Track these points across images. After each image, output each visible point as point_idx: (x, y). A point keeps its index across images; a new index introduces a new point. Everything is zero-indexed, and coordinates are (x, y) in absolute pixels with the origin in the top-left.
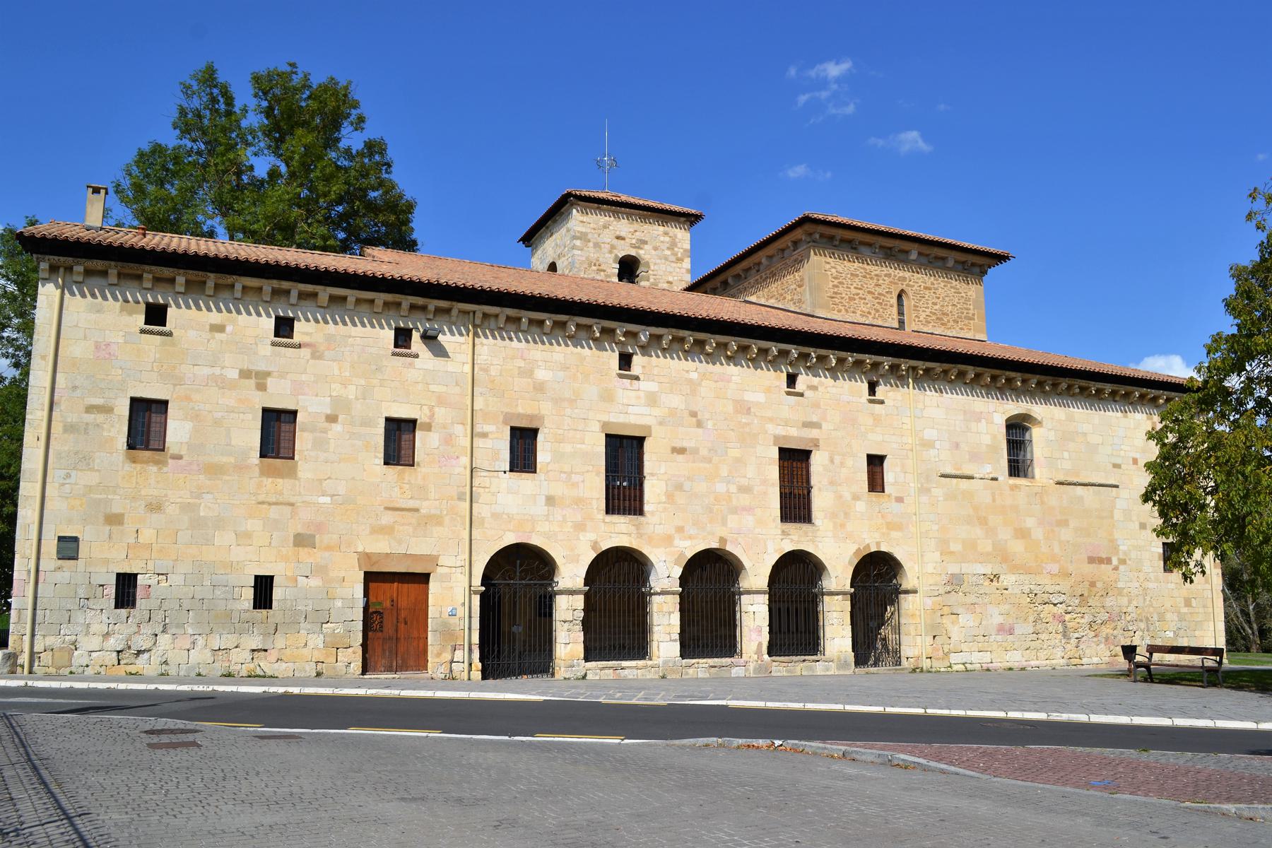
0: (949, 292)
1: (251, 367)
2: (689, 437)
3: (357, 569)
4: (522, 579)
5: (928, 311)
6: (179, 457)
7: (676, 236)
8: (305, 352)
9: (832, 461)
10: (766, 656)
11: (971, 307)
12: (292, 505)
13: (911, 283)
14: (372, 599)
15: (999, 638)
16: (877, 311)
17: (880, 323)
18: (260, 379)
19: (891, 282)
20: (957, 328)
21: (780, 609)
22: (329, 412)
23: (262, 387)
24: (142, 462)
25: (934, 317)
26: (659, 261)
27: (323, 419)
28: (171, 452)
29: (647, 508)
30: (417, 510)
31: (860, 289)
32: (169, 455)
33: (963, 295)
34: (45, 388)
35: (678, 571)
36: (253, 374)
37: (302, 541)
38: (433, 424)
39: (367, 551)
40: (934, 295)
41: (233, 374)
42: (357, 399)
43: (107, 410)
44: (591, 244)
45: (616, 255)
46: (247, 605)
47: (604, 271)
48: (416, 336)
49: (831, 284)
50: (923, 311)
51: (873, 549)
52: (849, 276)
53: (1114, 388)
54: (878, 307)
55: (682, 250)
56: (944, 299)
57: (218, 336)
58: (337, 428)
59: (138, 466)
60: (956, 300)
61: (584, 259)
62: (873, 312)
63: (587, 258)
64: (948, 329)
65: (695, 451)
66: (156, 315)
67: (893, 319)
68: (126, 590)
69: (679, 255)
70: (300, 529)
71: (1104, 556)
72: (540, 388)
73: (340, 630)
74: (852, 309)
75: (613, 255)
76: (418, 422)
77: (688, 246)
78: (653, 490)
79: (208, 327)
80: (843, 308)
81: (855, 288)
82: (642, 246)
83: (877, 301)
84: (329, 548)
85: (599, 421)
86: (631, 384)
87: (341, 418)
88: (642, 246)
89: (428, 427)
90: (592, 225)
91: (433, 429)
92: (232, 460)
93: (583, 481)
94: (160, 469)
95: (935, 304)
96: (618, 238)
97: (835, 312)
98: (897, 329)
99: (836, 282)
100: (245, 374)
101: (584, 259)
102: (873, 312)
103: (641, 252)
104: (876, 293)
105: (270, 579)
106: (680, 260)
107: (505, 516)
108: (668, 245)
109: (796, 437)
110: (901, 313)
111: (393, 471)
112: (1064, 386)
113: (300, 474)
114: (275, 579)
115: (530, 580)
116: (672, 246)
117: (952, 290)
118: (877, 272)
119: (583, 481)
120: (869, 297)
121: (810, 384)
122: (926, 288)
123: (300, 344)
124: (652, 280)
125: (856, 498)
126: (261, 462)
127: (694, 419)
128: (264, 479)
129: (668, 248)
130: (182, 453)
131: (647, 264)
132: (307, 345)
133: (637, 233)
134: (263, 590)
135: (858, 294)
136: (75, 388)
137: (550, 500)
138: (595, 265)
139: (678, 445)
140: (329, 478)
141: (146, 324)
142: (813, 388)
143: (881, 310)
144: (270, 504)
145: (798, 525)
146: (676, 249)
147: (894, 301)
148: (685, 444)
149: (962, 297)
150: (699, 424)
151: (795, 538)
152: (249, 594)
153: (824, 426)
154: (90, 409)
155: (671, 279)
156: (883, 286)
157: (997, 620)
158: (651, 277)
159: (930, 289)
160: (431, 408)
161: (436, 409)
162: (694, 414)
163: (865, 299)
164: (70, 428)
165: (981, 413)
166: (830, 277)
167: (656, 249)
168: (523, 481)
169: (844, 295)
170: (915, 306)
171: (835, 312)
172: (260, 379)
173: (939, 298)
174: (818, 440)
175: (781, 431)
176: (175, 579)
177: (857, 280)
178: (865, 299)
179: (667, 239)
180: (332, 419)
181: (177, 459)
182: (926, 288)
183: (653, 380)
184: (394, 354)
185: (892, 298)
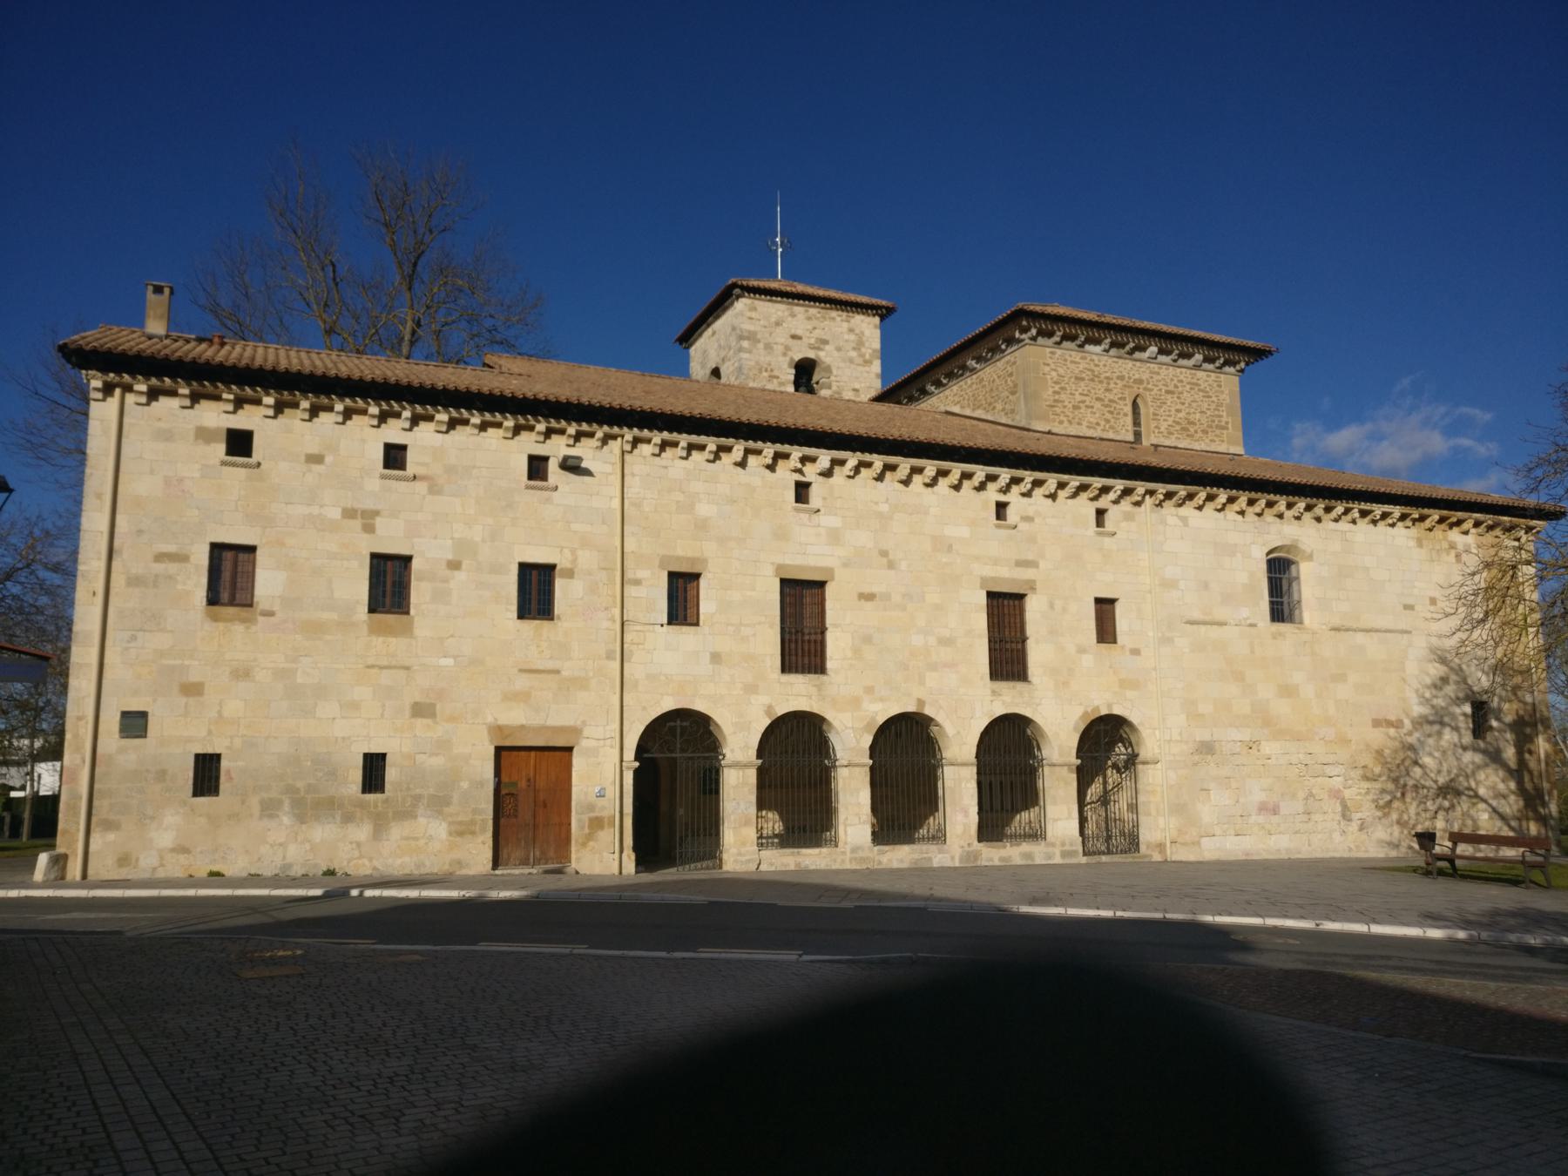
0: (1196, 396)
2: (878, 580)
4: (683, 750)
5: (1171, 419)
6: (270, 614)
7: (862, 333)
8: (421, 487)
9: (1052, 606)
11: (1225, 414)
12: (407, 668)
13: (1150, 386)
14: (505, 779)
15: (1261, 819)
16: (1108, 421)
18: (368, 520)
19: (1125, 386)
20: (1207, 441)
21: (991, 784)
22: (450, 557)
23: (369, 529)
25: (1178, 428)
26: (842, 365)
29: (829, 665)
30: (557, 672)
31: (1087, 395)
32: (258, 611)
33: (1214, 399)
34: (102, 532)
35: (868, 740)
36: (359, 512)
37: (422, 710)
38: (576, 570)
39: (500, 723)
40: (1178, 401)
41: (335, 513)
42: (483, 541)
43: (181, 558)
44: (761, 346)
45: (792, 359)
48: (553, 466)
49: (1051, 390)
50: (1165, 420)
51: (1104, 712)
52: (1073, 380)
53: (1404, 511)
54: (1108, 416)
56: (1190, 404)
57: (317, 468)
58: (460, 576)
59: (221, 625)
60: (1206, 405)
61: (752, 363)
62: (1103, 423)
63: (757, 363)
64: (1196, 441)
65: (887, 597)
66: (239, 443)
67: (1127, 431)
68: (207, 773)
69: (867, 357)
70: (418, 699)
71: (1393, 718)
72: (702, 525)
75: (788, 359)
76: (558, 568)
77: (877, 345)
78: (837, 645)
79: (303, 458)
80: (1065, 419)
81: (1081, 394)
82: (822, 346)
83: (1108, 409)
84: (452, 719)
85: (773, 564)
86: (810, 520)
88: (822, 346)
89: (570, 574)
90: (762, 322)
91: (576, 576)
92: (334, 616)
93: (754, 635)
94: (248, 628)
95: (1178, 411)
96: (794, 337)
97: (1056, 424)
98: (1132, 443)
99: (1057, 388)
100: (349, 513)
101: (752, 363)
103: (822, 354)
104: (1106, 400)
105: (382, 757)
106: (867, 362)
107: (663, 678)
108: (854, 345)
109: (1007, 577)
110: (1137, 423)
111: (530, 626)
112: (1340, 509)
113: (417, 632)
115: (694, 752)
116: (859, 345)
117: (1201, 394)
118: (1108, 375)
119: (754, 635)
120: (1098, 405)
122: (1168, 392)
123: (415, 477)
124: (834, 388)
125: (1082, 650)
126: (369, 618)
127: (885, 560)
128: (374, 638)
129: (854, 349)
130: (274, 609)
131: (828, 369)
132: (424, 478)
133: (817, 331)
134: (374, 770)
135: (1083, 402)
136: (140, 532)
137: (716, 658)
138: (766, 371)
139: (867, 590)
140: (452, 636)
142: (1028, 519)
143: (1113, 420)
144: (381, 668)
145: (1011, 684)
146: (863, 350)
147: (1128, 409)
148: (875, 589)
149: (1213, 402)
150: (891, 565)
151: (1008, 699)
152: (357, 775)
153: (1042, 564)
154: (160, 557)
156: (1115, 391)
157: (1258, 796)
160: (573, 552)
161: (580, 553)
162: (884, 554)
163: (1092, 407)
164: (134, 581)
165: (1236, 545)
166: (1050, 382)
167: (839, 349)
168: (683, 634)
169: (1066, 403)
170: (1155, 414)
171: (1056, 424)
172: (368, 520)
173: (1183, 404)
174: (1034, 581)
175: (989, 571)
177: (1082, 384)
178: (1092, 407)
179: (852, 337)
180: (454, 565)
182: (1168, 392)
183: (836, 515)
184: (528, 487)
185: (1126, 405)
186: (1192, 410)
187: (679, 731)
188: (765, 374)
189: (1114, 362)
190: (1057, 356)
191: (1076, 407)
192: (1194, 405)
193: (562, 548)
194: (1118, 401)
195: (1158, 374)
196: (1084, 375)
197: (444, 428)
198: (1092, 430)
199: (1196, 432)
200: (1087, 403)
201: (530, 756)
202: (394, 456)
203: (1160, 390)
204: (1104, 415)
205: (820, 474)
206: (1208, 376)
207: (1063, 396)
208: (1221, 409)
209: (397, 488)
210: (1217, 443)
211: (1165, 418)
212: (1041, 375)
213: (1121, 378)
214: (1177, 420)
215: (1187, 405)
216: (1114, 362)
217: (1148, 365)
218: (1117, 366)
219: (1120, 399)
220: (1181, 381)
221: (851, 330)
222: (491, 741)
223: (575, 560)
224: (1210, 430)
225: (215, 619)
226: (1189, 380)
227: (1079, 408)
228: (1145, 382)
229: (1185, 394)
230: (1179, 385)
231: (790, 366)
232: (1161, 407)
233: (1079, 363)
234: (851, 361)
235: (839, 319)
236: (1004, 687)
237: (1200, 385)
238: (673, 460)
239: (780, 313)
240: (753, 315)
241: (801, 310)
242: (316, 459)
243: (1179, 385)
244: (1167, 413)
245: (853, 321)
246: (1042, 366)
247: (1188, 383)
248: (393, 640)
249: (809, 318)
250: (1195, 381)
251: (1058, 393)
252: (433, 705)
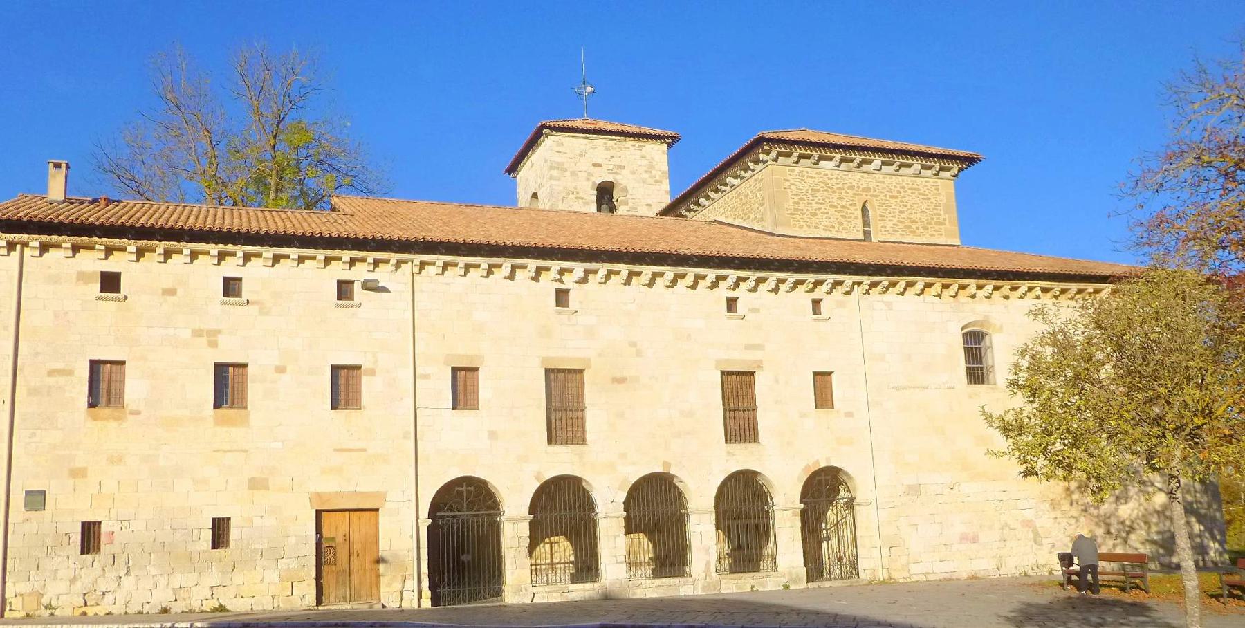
0: (917, 199)
1: (202, 327)
4: (469, 509)
5: (895, 220)
6: (137, 413)
10: (714, 574)
11: (942, 212)
12: (246, 451)
13: (876, 193)
14: (326, 534)
16: (841, 224)
17: (844, 236)
18: (211, 336)
20: (928, 235)
21: (738, 526)
22: (277, 363)
23: (213, 344)
24: (103, 419)
25: (901, 226)
28: (130, 408)
29: (588, 437)
30: (365, 450)
31: (821, 204)
33: (933, 200)
34: (9, 355)
35: (622, 496)
37: (256, 484)
40: (901, 204)
41: (187, 334)
43: (69, 373)
44: (568, 174)
45: (594, 183)
46: (206, 545)
47: (582, 199)
48: (357, 287)
50: (890, 220)
51: (823, 465)
52: (810, 191)
54: (842, 220)
55: (660, 173)
57: (171, 299)
59: (99, 423)
60: (926, 206)
61: (561, 188)
62: (837, 226)
64: (917, 236)
66: (110, 282)
67: (858, 231)
68: (90, 536)
69: (658, 178)
73: (294, 564)
74: (814, 225)
75: (591, 183)
78: (594, 420)
79: (160, 291)
80: (804, 224)
81: (817, 203)
82: (619, 171)
83: (841, 214)
86: (569, 319)
87: (289, 369)
88: (619, 171)
89: (372, 372)
94: (120, 424)
95: (902, 212)
96: (595, 165)
97: (797, 229)
98: (861, 241)
99: (796, 199)
100: (197, 333)
101: (561, 188)
102: (837, 226)
103: (619, 177)
106: (659, 182)
110: (866, 223)
111: (340, 414)
112: (1023, 289)
115: (478, 511)
117: (921, 197)
118: (839, 186)
120: (832, 211)
121: (751, 307)
122: (892, 197)
123: (248, 302)
124: (631, 204)
125: (803, 415)
129: (646, 172)
131: (625, 189)
132: (255, 303)
134: (220, 532)
135: (820, 209)
136: (37, 354)
138: (573, 193)
139: (618, 375)
140: (280, 425)
141: (101, 291)
142: (755, 310)
143: (845, 223)
144: (225, 452)
145: (743, 446)
146: (654, 172)
147: (859, 213)
149: (932, 203)
151: (741, 458)
154: (52, 373)
155: (649, 202)
158: (629, 201)
159: (896, 197)
162: (633, 344)
163: (827, 213)
164: (33, 392)
167: (633, 173)
169: (805, 211)
170: (881, 216)
171: (797, 229)
173: (906, 206)
176: (138, 525)
177: (818, 194)
178: (827, 213)
179: (644, 162)
180: (281, 370)
182: (892, 197)
184: (337, 306)
185: (856, 210)
186: (914, 211)
187: (465, 494)
188: (572, 197)
189: (845, 175)
190: (795, 173)
191: (814, 214)
192: (915, 206)
193: (365, 352)
194: (849, 207)
195: (883, 182)
196: (819, 187)
197: (270, 263)
198: (828, 232)
199: (918, 228)
200: (823, 210)
201: (345, 516)
202: (231, 287)
203: (885, 196)
204: (837, 219)
206: (926, 182)
207: (802, 206)
208: (939, 208)
209: (234, 311)
210: (936, 236)
211: (891, 218)
212: (783, 189)
213: (852, 188)
214: (900, 219)
215: (909, 207)
216: (845, 175)
217: (874, 175)
218: (847, 177)
219: (851, 205)
220: (904, 187)
221: (643, 157)
222: (312, 507)
224: (929, 226)
225: (95, 418)
226: (910, 186)
227: (816, 214)
228: (872, 190)
229: (907, 197)
230: (901, 190)
231: (592, 188)
232: (886, 210)
233: (815, 178)
234: (644, 182)
235: (632, 148)
236: (560, 450)
237: (920, 190)
238: (454, 277)
239: (583, 147)
240: (560, 149)
241: (599, 142)
242: (171, 292)
243: (901, 190)
244: (892, 214)
245: (644, 149)
246: (783, 181)
247: (909, 189)
248: (233, 429)
249: (608, 149)
250: (915, 186)
251: (797, 203)
252: (267, 480)
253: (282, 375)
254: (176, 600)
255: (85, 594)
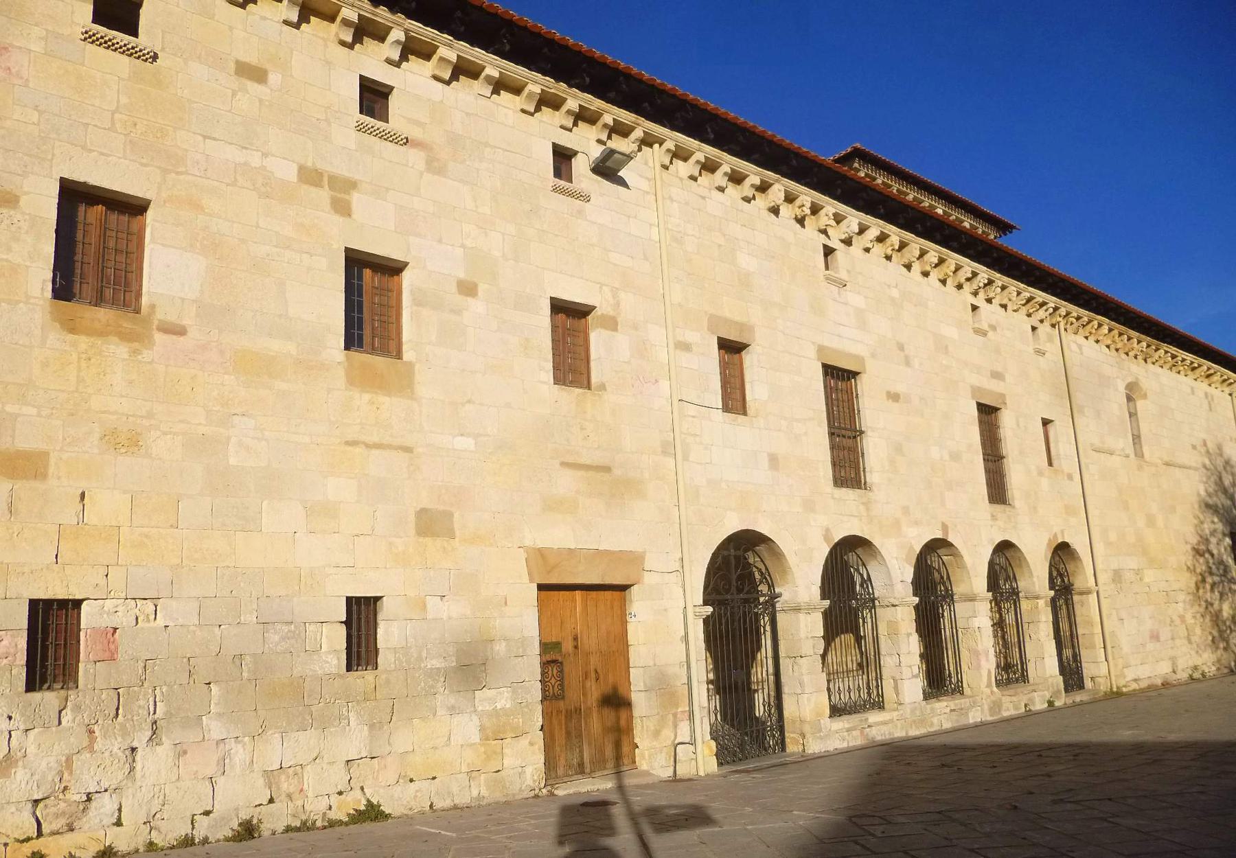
1: (321, 165)
3: (526, 578)
6: (179, 331)
8: (414, 157)
12: (408, 450)
22: (462, 275)
23: (342, 208)
24: (90, 332)
27: (454, 289)
28: (159, 315)
32: (156, 323)
36: (326, 179)
38: (619, 320)
46: (335, 662)
48: (581, 166)
57: (252, 87)
58: (476, 306)
59: (83, 341)
70: (426, 503)
85: (813, 343)
87: (482, 288)
89: (611, 324)
92: (291, 348)
93: (806, 434)
94: (135, 352)
100: (310, 176)
107: (724, 485)
113: (422, 390)
114: (386, 611)
126: (348, 358)
130: (186, 322)
132: (418, 145)
140: (469, 401)
144: (367, 446)
150: (908, 362)
160: (615, 291)
161: (622, 295)
176: (178, 612)
181: (175, 333)
183: (859, 293)
193: (602, 285)
197: (447, 75)
201: (574, 601)
205: (840, 240)
222: (531, 581)
223: (617, 305)
225: (71, 327)
238: (710, 189)
242: (253, 73)
248: (384, 400)
253: (469, 299)
254: (271, 801)
255: (36, 802)
